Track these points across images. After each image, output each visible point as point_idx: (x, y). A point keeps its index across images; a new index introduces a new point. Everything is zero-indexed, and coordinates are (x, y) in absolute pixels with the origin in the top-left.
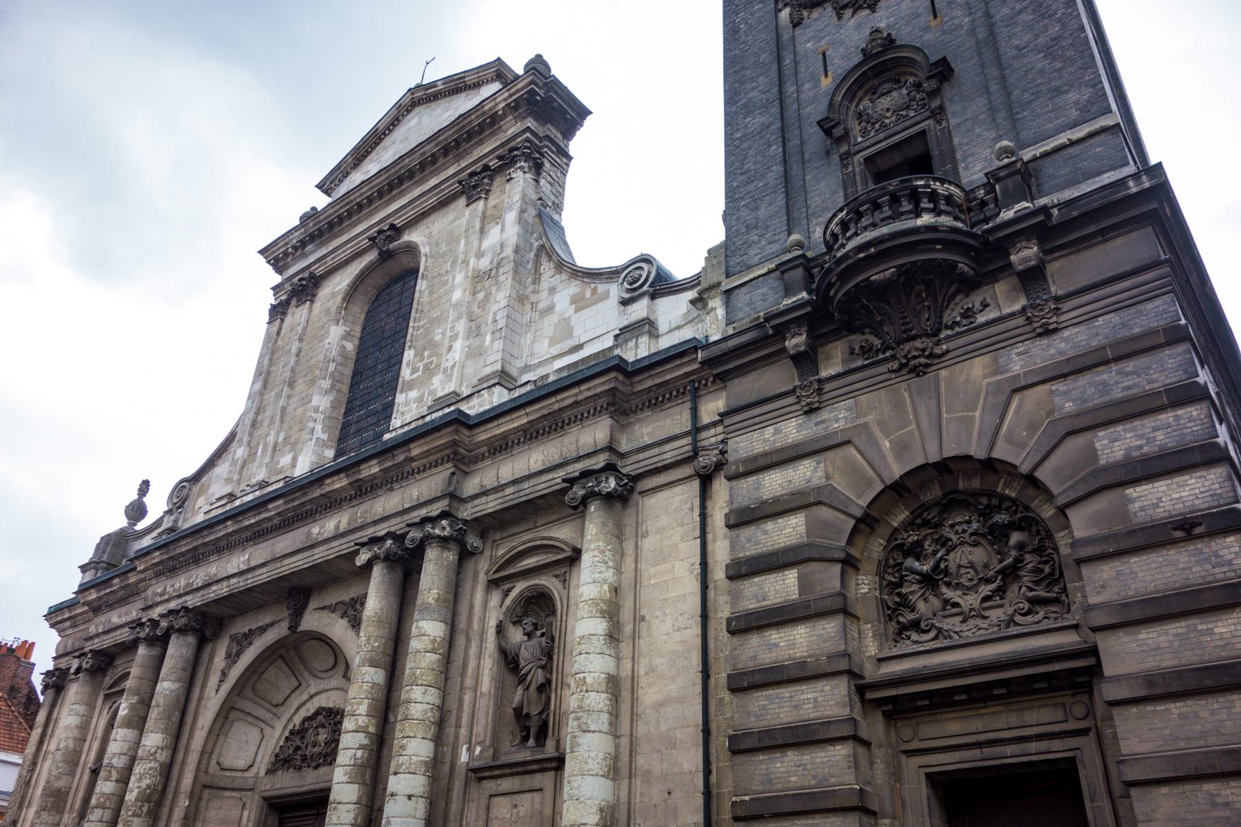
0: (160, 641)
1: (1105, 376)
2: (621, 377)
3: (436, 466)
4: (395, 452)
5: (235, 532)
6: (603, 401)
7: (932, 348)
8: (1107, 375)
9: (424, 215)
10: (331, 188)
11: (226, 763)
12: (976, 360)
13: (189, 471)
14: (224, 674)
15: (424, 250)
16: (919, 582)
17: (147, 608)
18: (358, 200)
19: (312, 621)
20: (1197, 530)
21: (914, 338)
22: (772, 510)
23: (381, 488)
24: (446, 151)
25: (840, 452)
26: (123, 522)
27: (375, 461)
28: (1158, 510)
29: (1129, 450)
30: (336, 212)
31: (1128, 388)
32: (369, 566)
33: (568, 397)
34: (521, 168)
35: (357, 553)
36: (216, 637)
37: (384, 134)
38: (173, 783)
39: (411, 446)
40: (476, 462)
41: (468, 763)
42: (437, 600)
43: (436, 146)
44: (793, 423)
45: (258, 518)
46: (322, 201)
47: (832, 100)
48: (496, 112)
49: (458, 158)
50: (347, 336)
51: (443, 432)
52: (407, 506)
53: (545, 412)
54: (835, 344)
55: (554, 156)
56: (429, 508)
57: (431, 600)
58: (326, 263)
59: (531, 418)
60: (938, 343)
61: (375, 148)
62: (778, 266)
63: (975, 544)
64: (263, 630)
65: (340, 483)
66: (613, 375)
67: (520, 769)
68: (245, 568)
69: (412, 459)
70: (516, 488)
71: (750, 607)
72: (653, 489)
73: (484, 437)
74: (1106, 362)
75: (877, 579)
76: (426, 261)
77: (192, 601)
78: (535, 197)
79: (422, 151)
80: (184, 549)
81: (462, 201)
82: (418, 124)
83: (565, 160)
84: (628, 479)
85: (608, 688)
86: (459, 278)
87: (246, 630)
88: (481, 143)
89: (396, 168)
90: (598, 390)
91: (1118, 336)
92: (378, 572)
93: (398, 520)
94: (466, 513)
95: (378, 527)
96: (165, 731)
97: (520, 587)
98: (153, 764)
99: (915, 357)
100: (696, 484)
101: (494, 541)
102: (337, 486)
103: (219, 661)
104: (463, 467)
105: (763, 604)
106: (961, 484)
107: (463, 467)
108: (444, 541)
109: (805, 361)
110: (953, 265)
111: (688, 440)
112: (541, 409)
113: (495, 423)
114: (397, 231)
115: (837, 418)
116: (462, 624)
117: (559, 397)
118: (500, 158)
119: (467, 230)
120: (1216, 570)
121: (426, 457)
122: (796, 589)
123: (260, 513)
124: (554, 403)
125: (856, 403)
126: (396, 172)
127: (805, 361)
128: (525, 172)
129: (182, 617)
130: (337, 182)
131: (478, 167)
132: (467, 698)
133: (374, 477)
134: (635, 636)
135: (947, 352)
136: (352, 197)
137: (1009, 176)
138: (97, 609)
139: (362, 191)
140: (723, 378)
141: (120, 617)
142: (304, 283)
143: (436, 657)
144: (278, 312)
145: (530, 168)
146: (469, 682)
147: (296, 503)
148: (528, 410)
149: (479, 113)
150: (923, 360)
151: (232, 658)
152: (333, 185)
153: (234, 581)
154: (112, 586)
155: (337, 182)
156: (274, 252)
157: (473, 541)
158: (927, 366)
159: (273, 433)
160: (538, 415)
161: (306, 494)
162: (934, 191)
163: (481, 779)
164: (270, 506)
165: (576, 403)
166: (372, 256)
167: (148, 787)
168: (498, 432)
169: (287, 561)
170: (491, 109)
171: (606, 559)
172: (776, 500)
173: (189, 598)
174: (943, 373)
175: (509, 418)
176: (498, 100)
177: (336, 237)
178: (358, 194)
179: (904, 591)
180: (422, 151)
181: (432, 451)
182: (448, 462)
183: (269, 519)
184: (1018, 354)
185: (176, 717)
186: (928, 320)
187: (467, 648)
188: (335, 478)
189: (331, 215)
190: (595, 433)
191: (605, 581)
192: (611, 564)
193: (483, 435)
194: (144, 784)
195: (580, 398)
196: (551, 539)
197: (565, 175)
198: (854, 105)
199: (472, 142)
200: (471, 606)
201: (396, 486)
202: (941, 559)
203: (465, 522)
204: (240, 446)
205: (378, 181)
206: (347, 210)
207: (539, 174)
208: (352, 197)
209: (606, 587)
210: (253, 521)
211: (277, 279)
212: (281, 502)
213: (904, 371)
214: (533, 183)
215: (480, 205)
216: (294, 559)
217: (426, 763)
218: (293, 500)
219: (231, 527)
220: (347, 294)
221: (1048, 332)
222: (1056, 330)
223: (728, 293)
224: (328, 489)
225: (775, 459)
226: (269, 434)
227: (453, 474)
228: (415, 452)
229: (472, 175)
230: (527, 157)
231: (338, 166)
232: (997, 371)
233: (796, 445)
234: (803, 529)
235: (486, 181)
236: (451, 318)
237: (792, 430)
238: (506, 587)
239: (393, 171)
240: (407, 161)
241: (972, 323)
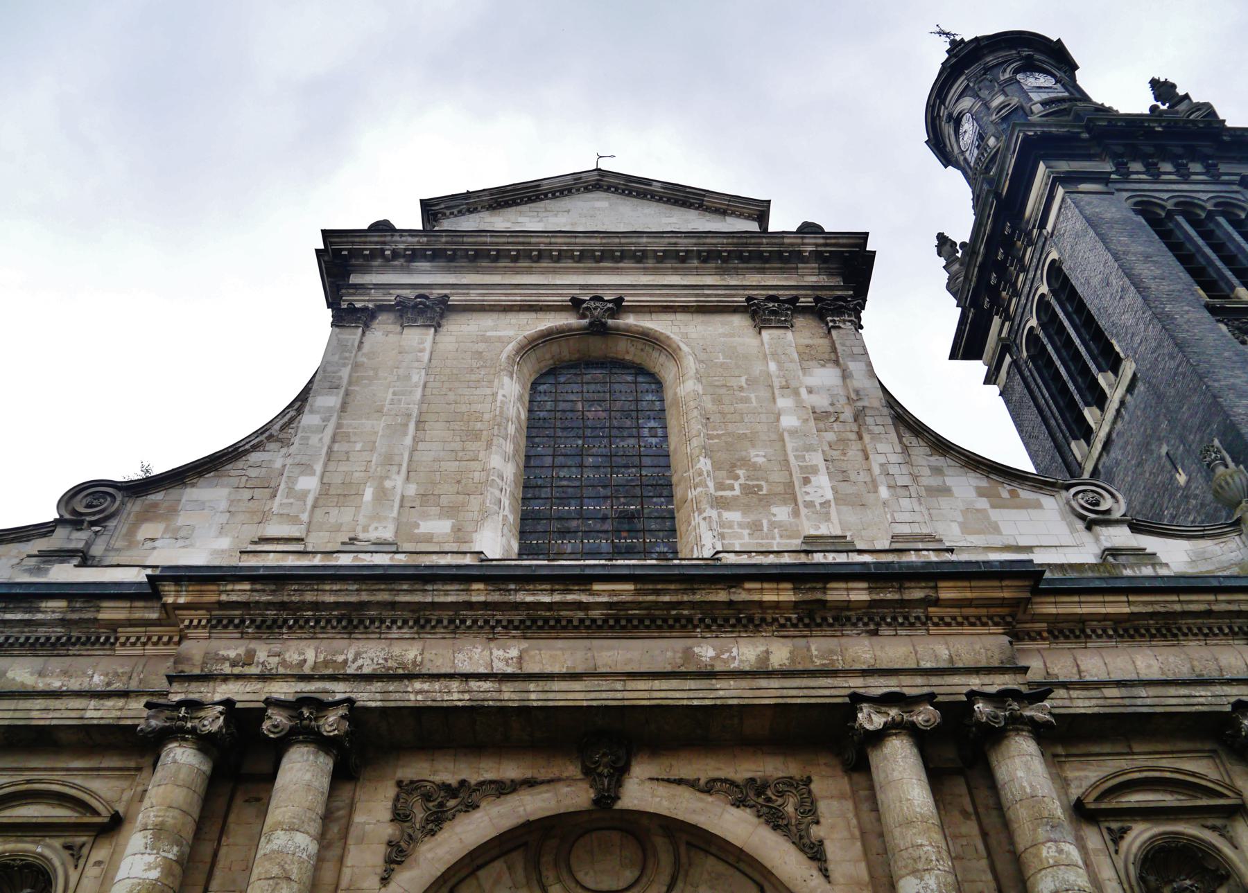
5: (485, 605)
10: (444, 214)
23: (855, 625)
33: (1197, 603)
37: (546, 195)
45: (557, 598)
46: (409, 219)
53: (1158, 608)
56: (987, 679)
69: (937, 602)
70: (1124, 692)
73: (1052, 610)
80: (330, 599)
93: (919, 680)
95: (871, 681)
112: (1152, 603)
117: (1183, 598)
121: (960, 607)
123: (570, 591)
124: (1173, 602)
133: (848, 605)
136: (533, 240)
139: (553, 240)
152: (448, 212)
155: (455, 211)
156: (353, 243)
161: (693, 591)
164: (597, 587)
165: (1209, 613)
168: (1079, 611)
176: (806, 241)
177: (478, 272)
178: (547, 240)
181: (975, 602)
193: (1049, 607)
201: (884, 630)
208: (533, 240)
210: (546, 599)
212: (630, 587)
219: (479, 593)
228: (945, 594)
231: (468, 194)
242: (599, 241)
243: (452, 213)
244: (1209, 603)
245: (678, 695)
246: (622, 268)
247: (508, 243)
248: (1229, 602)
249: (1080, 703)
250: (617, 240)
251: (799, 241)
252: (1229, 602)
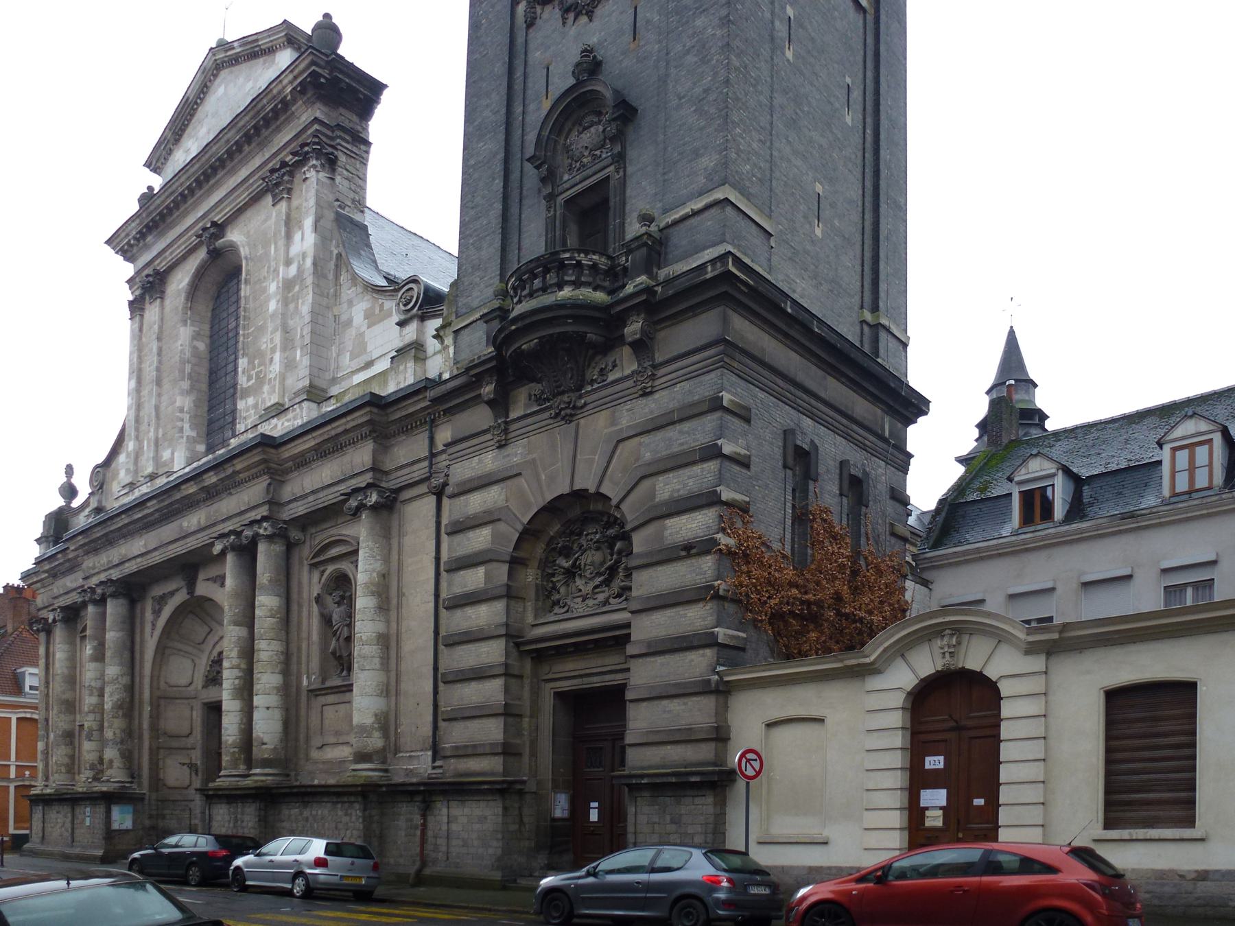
0: (102, 602)
1: (671, 434)
2: (375, 410)
3: (257, 477)
4: (225, 466)
6: (365, 430)
7: (575, 402)
8: (671, 433)
9: (241, 211)
11: (173, 681)
12: (602, 412)
13: (101, 458)
14: (154, 625)
15: (244, 252)
16: (564, 574)
17: (85, 578)
18: (180, 190)
19: (202, 589)
20: (694, 551)
21: (563, 393)
22: (473, 523)
24: (248, 138)
25: (515, 481)
26: (60, 502)
27: (212, 473)
28: (679, 536)
29: (673, 491)
30: (163, 202)
31: (682, 444)
32: (223, 553)
34: (314, 166)
35: (212, 544)
36: (142, 598)
38: (137, 696)
39: (235, 462)
40: (287, 474)
41: (308, 686)
42: (270, 581)
43: (238, 132)
44: (490, 455)
46: (157, 182)
47: (539, 135)
48: (285, 97)
49: (262, 146)
50: (196, 336)
51: (254, 452)
52: (243, 509)
53: (326, 437)
54: (520, 390)
55: (349, 146)
57: (265, 581)
58: (166, 258)
59: (317, 441)
60: (580, 397)
61: (191, 120)
62: (482, 317)
63: (598, 549)
64: (172, 593)
65: (191, 489)
66: (368, 409)
67: (336, 690)
68: (145, 550)
69: (239, 472)
71: (458, 591)
72: (409, 499)
73: (287, 455)
74: (673, 423)
75: (539, 572)
76: (247, 265)
77: (115, 574)
78: (331, 198)
79: (226, 138)
80: (98, 535)
81: (269, 199)
82: (225, 93)
83: (363, 147)
84: (391, 493)
85: (378, 642)
86: (273, 287)
87: (161, 593)
88: (278, 130)
89: (207, 156)
90: (360, 421)
91: (686, 401)
92: (230, 558)
93: (238, 519)
94: (287, 513)
96: (121, 664)
97: (330, 568)
98: (117, 686)
99: (562, 409)
100: (432, 499)
101: (312, 534)
102: (191, 491)
103: (149, 616)
104: (278, 478)
105: (465, 589)
106: (591, 506)
107: (278, 478)
108: (270, 538)
109: (500, 404)
110: (582, 336)
111: (426, 463)
113: (293, 444)
114: (219, 229)
115: (517, 453)
116: (294, 596)
118: (294, 154)
119: (275, 234)
120: (698, 577)
122: (482, 580)
124: (330, 430)
125: (529, 442)
126: (208, 160)
127: (500, 404)
128: (318, 171)
129: (110, 586)
130: (163, 160)
131: (275, 163)
132: (304, 646)
133: (215, 485)
134: (399, 606)
135: (585, 404)
137: (638, 248)
138: (54, 575)
140: (450, 412)
141: (71, 582)
142: (151, 279)
143: (273, 620)
144: (136, 307)
145: (323, 166)
146: (304, 635)
147: (166, 503)
148: (314, 434)
149: (270, 96)
150: (569, 411)
151: (157, 613)
153: (139, 560)
154: (57, 560)
157: (295, 534)
158: (572, 415)
159: (152, 430)
160: (321, 439)
161: (170, 496)
162: (579, 263)
163: (317, 695)
165: (346, 431)
166: (202, 254)
167: (118, 700)
168: (296, 452)
169: (171, 547)
170: (279, 93)
171: (375, 554)
172: (475, 516)
173: (112, 571)
174: (582, 421)
175: (300, 441)
177: (171, 228)
178: (177, 184)
179: (554, 579)
180: (226, 138)
182: (264, 474)
183: (152, 514)
184: (628, 410)
185: (127, 655)
186: (571, 378)
187: (300, 612)
188: (188, 485)
189: (159, 206)
190: (361, 456)
191: (374, 570)
192: (378, 558)
194: (116, 697)
195: (348, 427)
196: (344, 535)
197: (365, 165)
198: (563, 138)
199: (270, 130)
200: (300, 583)
202: (577, 558)
203: (285, 522)
204: (130, 440)
205: (193, 170)
206: (173, 201)
207: (333, 170)
208: (174, 187)
209: (375, 575)
210: (140, 515)
211: (129, 269)
213: (559, 419)
214: (328, 181)
215: (283, 205)
216: (175, 546)
217: (277, 689)
218: (163, 501)
220: (189, 293)
221: (645, 394)
222: (651, 393)
223: (456, 332)
224: (185, 493)
225: (476, 484)
226: (149, 431)
227: (269, 484)
228: (239, 467)
229: (273, 171)
230: (319, 154)
232: (613, 423)
233: (489, 475)
234: (489, 538)
235: (286, 178)
236: (270, 329)
237: (489, 462)
238: (322, 569)
239: (204, 159)
240: (214, 149)
241: (604, 381)
242: (197, 166)
243: (162, 164)
244: (345, 424)
245: (179, 549)
246: (220, 179)
247: (167, 197)
248: (353, 420)
249: (301, 509)
250: (204, 159)
251: (280, 87)
252: (353, 420)
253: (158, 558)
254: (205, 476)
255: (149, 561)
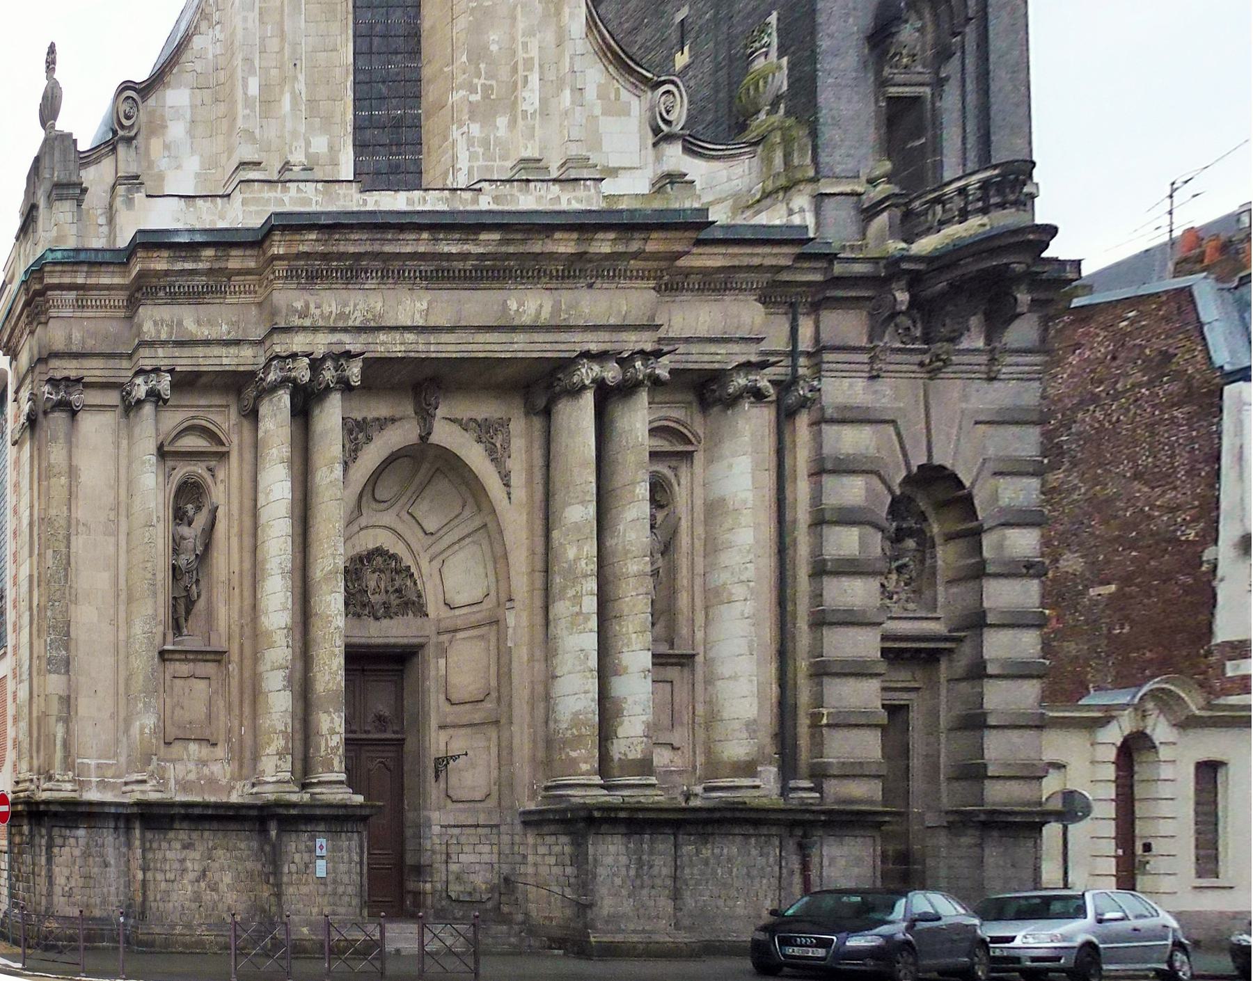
39: (654, 235)
153: (410, 337)
169: (481, 337)
188: (566, 236)
210: (454, 249)
216: (490, 337)
218: (507, 242)
253: (450, 348)
254: (600, 235)
255: (432, 348)
